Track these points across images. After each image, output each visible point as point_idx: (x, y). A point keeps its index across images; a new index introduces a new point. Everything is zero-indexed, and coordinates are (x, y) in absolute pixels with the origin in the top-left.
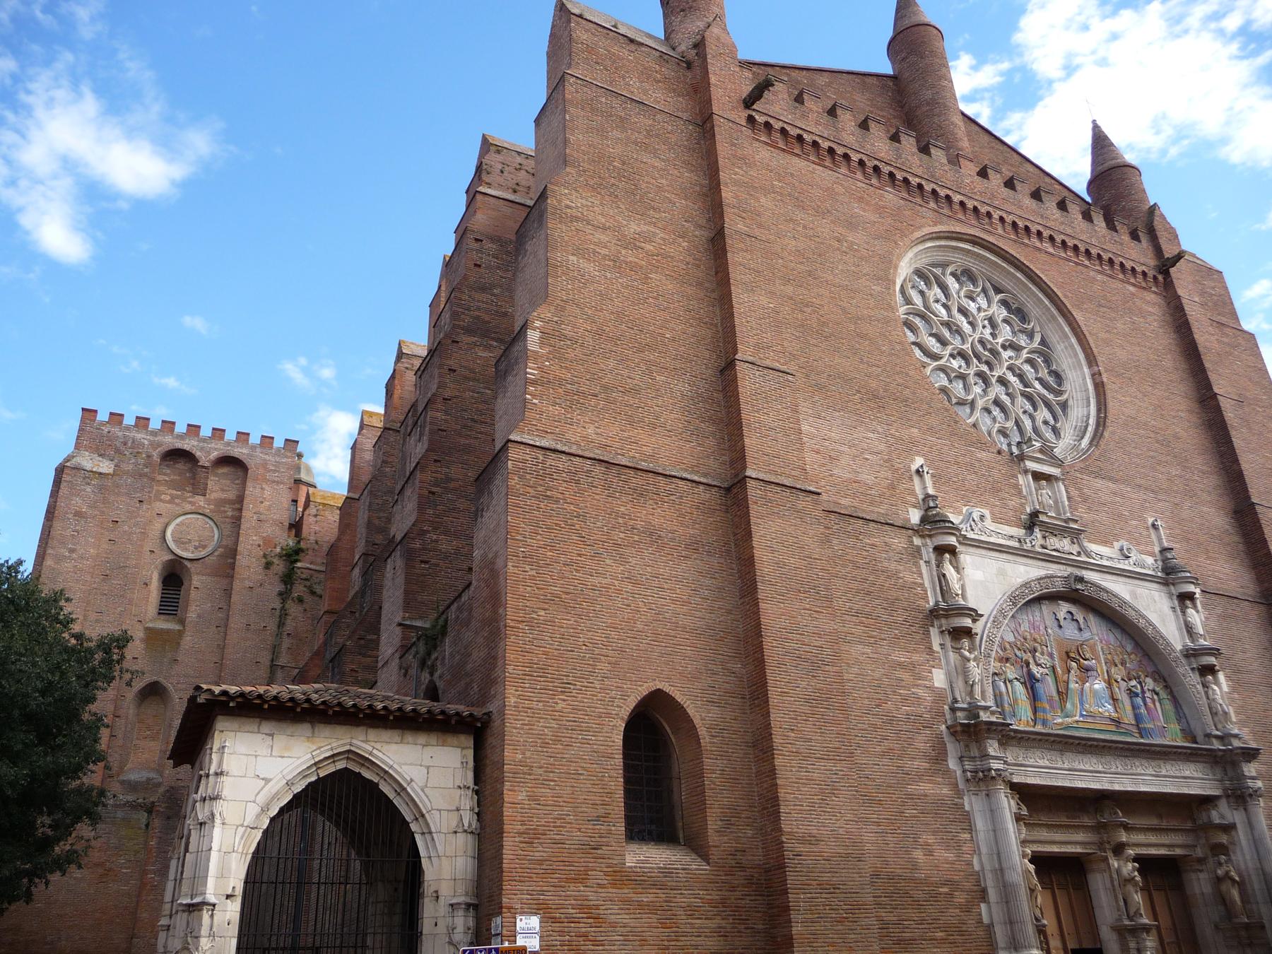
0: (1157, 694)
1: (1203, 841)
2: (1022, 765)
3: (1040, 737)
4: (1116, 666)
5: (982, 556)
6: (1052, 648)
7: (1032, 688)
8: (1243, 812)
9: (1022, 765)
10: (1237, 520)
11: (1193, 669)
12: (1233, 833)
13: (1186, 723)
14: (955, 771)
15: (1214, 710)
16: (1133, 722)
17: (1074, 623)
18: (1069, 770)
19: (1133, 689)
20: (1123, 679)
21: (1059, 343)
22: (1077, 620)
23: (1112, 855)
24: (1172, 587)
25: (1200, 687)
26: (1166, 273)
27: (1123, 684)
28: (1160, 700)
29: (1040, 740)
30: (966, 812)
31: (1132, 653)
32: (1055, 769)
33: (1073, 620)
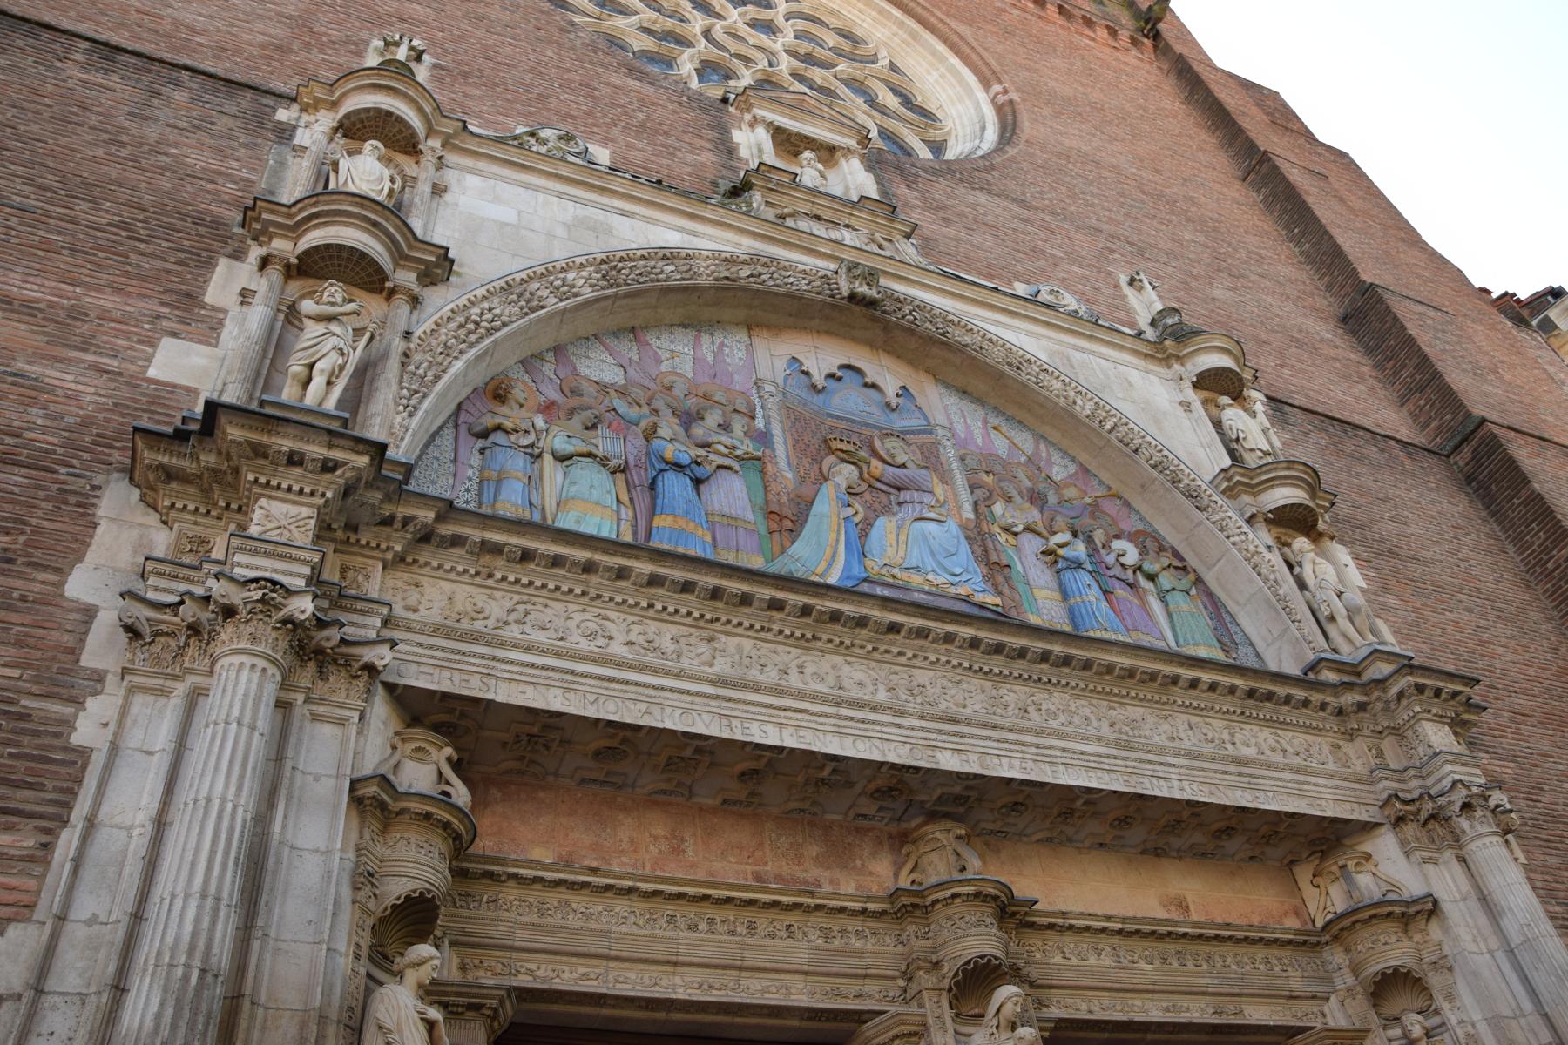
0: (1151, 578)
1: (1345, 980)
2: (475, 638)
3: (583, 555)
4: (1009, 500)
5: (527, 186)
6: (767, 418)
7: (652, 486)
8: (1456, 866)
9: (475, 638)
10: (1353, 333)
11: (1251, 520)
12: (1435, 931)
13: (1252, 655)
14: (89, 613)
15: (1324, 611)
16: (1068, 628)
17: (871, 392)
18: (724, 683)
19: (1061, 552)
20: (1027, 529)
21: (929, 73)
22: (874, 386)
23: (948, 1014)
24: (1177, 367)
25: (1275, 559)
26: (1156, 36)
27: (1032, 544)
28: (1162, 596)
29: (589, 568)
30: (67, 749)
31: (1067, 486)
32: (655, 671)
33: (866, 385)
